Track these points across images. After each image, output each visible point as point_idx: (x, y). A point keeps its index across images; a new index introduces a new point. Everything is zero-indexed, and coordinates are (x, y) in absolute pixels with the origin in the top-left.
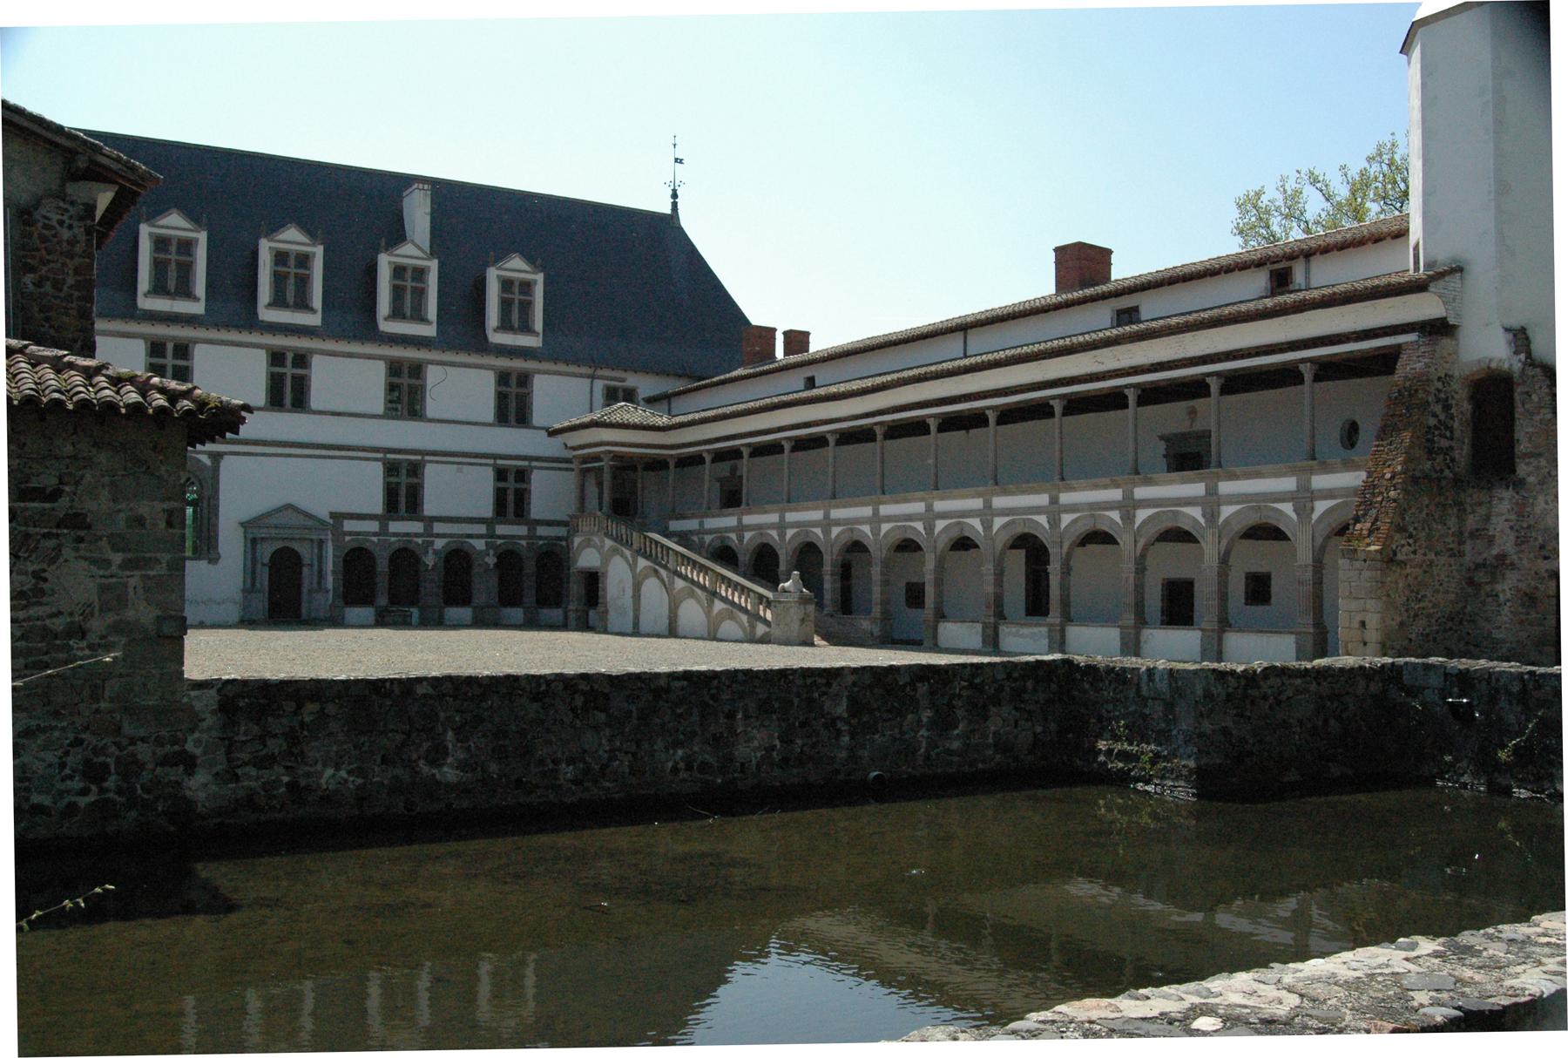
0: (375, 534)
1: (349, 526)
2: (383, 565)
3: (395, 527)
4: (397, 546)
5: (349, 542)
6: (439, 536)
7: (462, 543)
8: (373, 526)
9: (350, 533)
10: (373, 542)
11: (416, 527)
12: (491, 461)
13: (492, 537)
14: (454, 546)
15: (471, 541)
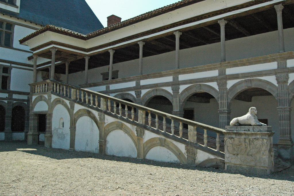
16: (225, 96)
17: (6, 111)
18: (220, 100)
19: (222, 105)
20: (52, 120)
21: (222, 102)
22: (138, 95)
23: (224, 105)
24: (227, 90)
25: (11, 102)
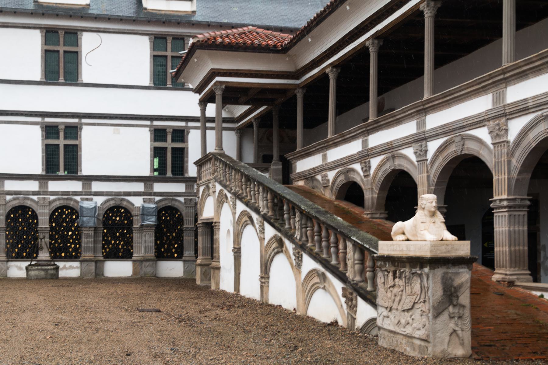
0: (34, 193)
1: (10, 185)
2: (44, 222)
3: (54, 186)
4: (58, 204)
5: (10, 201)
6: (97, 194)
7: (123, 200)
8: (33, 186)
9: (9, 193)
10: (32, 200)
11: (75, 186)
12: (148, 123)
13: (150, 194)
14: (112, 203)
15: (131, 199)
16: (504, 161)
17: (185, 218)
18: (496, 175)
19: (499, 185)
20: (219, 235)
21: (498, 179)
22: (366, 171)
23: (502, 187)
24: (509, 146)
25: (191, 199)
